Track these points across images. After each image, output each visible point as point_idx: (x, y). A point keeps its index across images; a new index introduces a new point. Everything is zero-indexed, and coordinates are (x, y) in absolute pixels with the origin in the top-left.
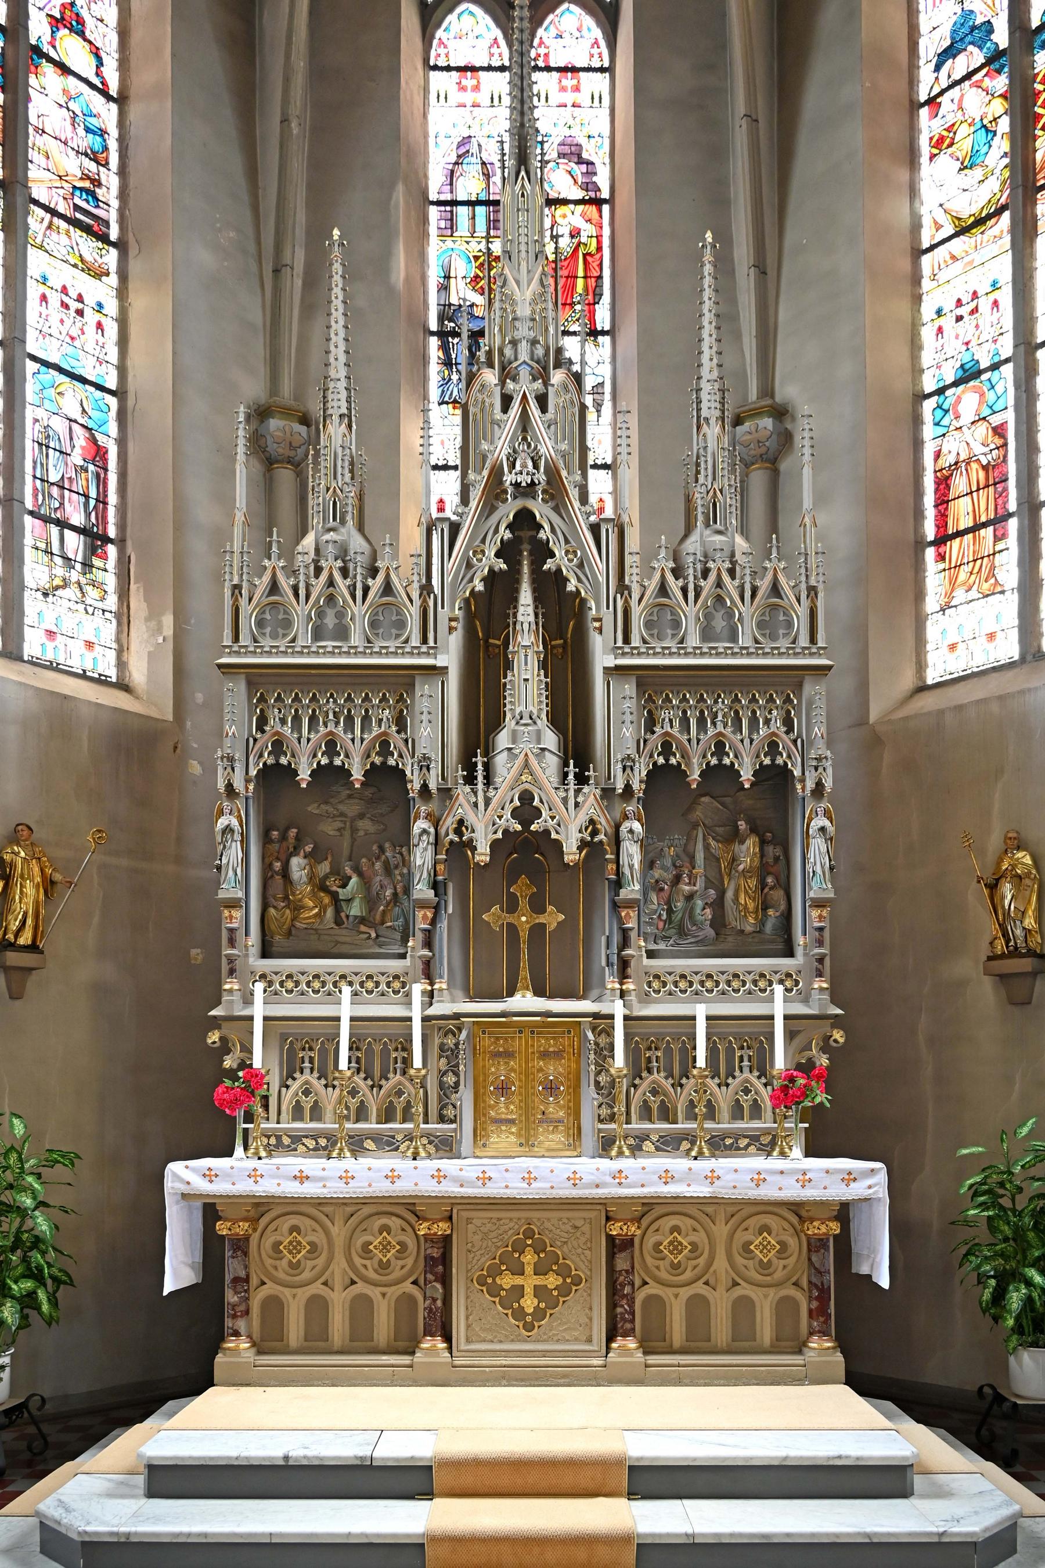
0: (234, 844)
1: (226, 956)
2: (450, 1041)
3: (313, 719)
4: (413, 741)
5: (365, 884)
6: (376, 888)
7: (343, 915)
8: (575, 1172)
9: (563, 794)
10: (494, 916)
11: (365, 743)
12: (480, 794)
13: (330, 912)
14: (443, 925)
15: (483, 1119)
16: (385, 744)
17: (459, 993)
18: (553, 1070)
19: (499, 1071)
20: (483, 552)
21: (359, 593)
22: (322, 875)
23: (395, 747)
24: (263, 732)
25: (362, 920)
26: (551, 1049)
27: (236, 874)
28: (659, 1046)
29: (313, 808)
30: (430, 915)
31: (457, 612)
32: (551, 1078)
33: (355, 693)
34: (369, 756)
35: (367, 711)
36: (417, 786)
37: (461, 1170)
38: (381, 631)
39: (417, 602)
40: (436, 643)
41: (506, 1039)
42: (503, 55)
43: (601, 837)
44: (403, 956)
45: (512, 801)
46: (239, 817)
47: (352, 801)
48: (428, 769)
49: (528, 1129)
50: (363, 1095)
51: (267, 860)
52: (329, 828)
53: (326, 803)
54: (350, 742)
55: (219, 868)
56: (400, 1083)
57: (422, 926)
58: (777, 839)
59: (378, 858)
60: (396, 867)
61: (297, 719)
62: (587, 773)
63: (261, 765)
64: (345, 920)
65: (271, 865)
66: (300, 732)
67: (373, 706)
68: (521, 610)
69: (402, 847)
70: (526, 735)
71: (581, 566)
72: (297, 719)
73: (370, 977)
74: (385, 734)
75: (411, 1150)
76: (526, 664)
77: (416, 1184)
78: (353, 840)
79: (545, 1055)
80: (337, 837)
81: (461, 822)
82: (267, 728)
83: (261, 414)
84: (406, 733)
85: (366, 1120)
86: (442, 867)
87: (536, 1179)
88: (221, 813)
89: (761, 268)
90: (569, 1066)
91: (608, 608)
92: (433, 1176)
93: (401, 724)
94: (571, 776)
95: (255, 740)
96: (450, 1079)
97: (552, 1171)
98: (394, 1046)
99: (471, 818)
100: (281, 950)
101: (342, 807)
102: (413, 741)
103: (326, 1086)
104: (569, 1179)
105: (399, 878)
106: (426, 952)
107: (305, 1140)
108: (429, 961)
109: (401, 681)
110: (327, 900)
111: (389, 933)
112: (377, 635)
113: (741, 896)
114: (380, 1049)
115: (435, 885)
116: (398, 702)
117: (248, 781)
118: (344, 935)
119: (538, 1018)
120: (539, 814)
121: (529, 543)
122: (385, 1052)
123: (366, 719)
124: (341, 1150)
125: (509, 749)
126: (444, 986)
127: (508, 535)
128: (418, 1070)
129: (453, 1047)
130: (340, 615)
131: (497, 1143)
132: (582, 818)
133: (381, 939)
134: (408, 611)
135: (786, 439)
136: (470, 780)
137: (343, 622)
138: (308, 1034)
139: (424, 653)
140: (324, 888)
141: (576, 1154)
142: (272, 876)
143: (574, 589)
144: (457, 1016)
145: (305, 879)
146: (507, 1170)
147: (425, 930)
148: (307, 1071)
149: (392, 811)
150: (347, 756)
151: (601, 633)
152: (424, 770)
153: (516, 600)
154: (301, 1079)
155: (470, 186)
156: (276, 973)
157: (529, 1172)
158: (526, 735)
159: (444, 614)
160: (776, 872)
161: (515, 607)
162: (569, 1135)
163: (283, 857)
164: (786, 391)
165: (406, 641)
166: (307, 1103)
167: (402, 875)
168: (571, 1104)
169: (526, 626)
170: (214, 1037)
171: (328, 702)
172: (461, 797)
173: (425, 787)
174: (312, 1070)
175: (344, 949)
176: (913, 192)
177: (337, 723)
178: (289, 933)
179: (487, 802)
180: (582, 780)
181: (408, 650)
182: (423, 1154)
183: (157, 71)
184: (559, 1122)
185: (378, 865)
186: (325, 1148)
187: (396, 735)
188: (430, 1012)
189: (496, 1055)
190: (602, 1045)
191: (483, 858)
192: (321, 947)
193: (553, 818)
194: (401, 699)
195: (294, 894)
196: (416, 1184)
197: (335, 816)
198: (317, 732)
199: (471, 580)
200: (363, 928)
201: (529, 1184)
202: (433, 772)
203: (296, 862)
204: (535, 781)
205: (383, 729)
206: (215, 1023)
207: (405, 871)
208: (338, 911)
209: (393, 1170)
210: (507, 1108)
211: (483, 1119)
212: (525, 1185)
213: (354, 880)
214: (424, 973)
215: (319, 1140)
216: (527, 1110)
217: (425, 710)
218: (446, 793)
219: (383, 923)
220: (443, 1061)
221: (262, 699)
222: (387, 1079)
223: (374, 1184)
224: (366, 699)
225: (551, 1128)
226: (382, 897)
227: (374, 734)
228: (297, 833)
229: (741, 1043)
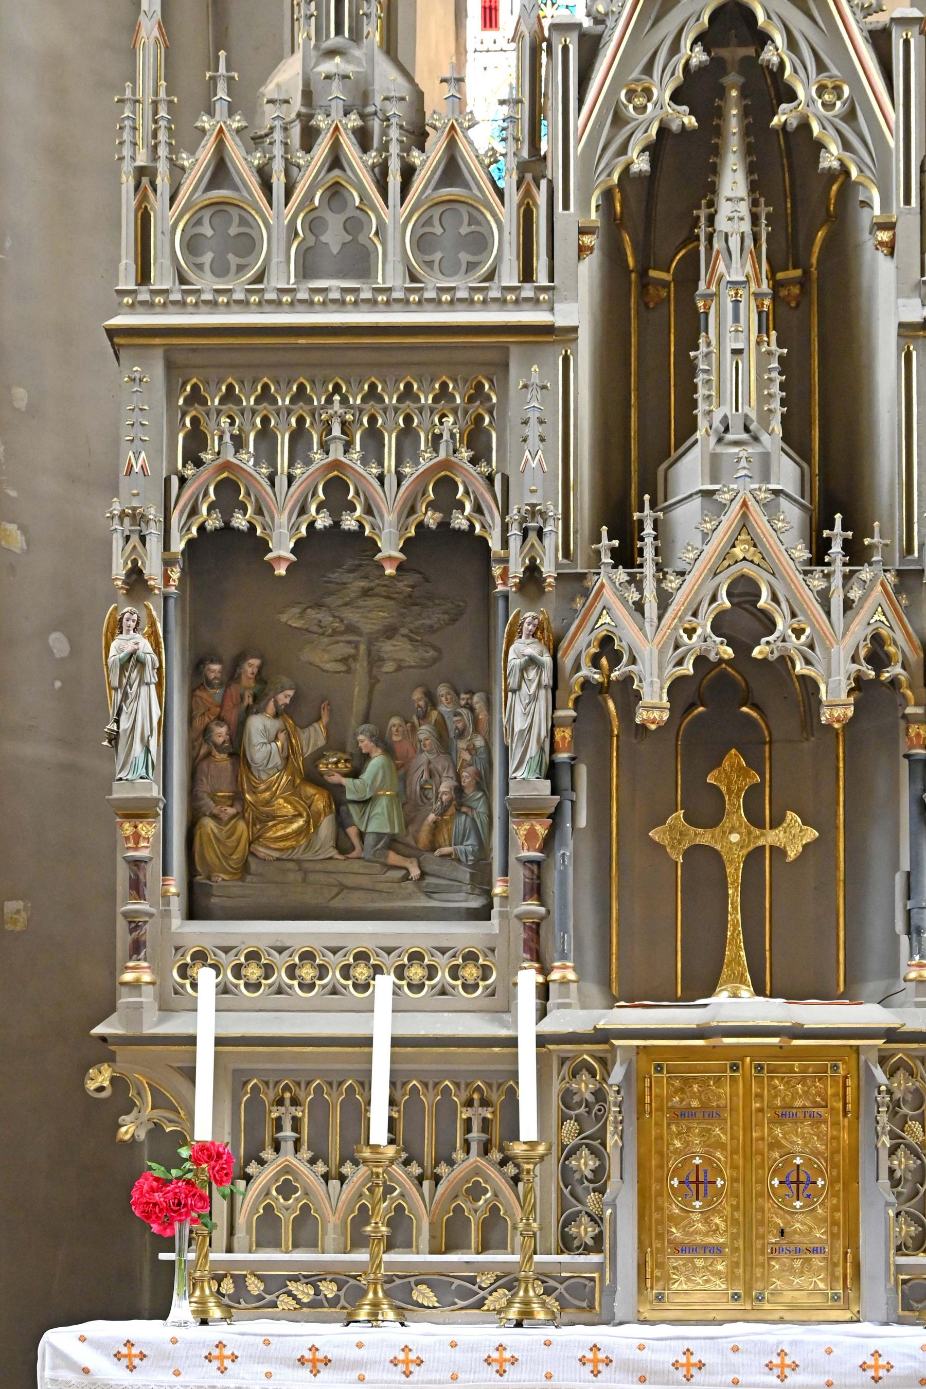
0: (144, 689)
1: (126, 915)
2: (585, 1087)
3: (299, 436)
4: (506, 480)
5: (398, 768)
6: (418, 776)
7: (352, 832)
8: (876, 1354)
9: (818, 583)
10: (674, 834)
11: (405, 484)
12: (650, 586)
13: (327, 826)
14: (566, 851)
15: (657, 1244)
16: (446, 486)
17: (593, 990)
18: (802, 1143)
19: (689, 1145)
20: (648, 92)
21: (394, 180)
22: (308, 751)
23: (467, 492)
24: (199, 463)
25: (392, 842)
26: (798, 1103)
27: (148, 751)
29: (291, 618)
30: (541, 830)
31: (593, 215)
32: (798, 1161)
33: (384, 382)
34: (412, 511)
35: (408, 419)
36: (517, 569)
37: (641, 1348)
38: (437, 256)
39: (513, 197)
40: (551, 280)
41: (704, 1082)
43: (895, 670)
44: (483, 914)
45: (714, 599)
46: (152, 636)
47: (371, 602)
48: (540, 533)
49: (749, 1265)
50: (402, 1195)
51: (199, 723)
52: (324, 657)
53: (319, 606)
54: (376, 483)
55: (114, 738)
56: (477, 1171)
57: (525, 854)
59: (424, 717)
60: (461, 734)
61: (266, 435)
62: (867, 541)
63: (194, 530)
64: (356, 840)
65: (206, 732)
66: (273, 463)
67: (421, 410)
68: (725, 209)
69: (472, 693)
70: (743, 463)
71: (850, 116)
72: (266, 435)
73: (416, 957)
74: (446, 464)
75: (516, 1307)
76: (736, 319)
77: (549, 1377)
78: (373, 680)
79: (784, 1115)
81: (607, 642)
82: (207, 457)
84: (489, 463)
85: (408, 1245)
86: (568, 733)
87: (795, 1367)
88: (117, 627)
90: (835, 1138)
91: (907, 201)
92: (583, 1361)
93: (477, 442)
94: (836, 548)
95: (183, 480)
96: (585, 1163)
97: (829, 1352)
98: (464, 1095)
99: (629, 634)
100: (228, 903)
101: (351, 615)
102: (506, 480)
103: (326, 1177)
104: (864, 1367)
105: (467, 756)
106: (533, 907)
107: (292, 1286)
108: (538, 925)
109: (479, 361)
110: (320, 802)
111: (446, 868)
112: (430, 264)
114: (455, 1099)
115: (551, 772)
116: (471, 399)
117: (168, 563)
118: (353, 869)
119: (775, 1041)
120: (770, 626)
121: (741, 72)
122: (445, 1110)
123: (407, 434)
124: (376, 1305)
125: (707, 494)
126: (571, 976)
127: (699, 57)
128: (532, 1145)
129: (591, 1098)
130: (354, 225)
131: (686, 1292)
132: (858, 633)
133: (430, 880)
134: (494, 215)
136: (626, 557)
137: (361, 239)
138: (287, 1072)
139: (527, 300)
140: (315, 779)
141: (848, 1315)
142: (209, 754)
143: (835, 164)
144: (603, 1036)
145: (277, 760)
146: (735, 1349)
147: (531, 862)
148: (288, 1146)
149: (453, 621)
150: (369, 511)
151: (891, 254)
152: (533, 536)
153: (713, 189)
154: (275, 1163)
156: (226, 950)
157: (782, 1354)
158: (743, 463)
159: (568, 220)
161: (711, 204)
162: (834, 1278)
163: (232, 715)
165: (490, 276)
166: (287, 1211)
167: (471, 750)
168: (839, 1215)
169: (734, 243)
170: (100, 1078)
171: (329, 401)
172: (608, 592)
173: (533, 571)
174: (297, 1144)
175: (357, 901)
177: (348, 447)
178: (245, 869)
179: (664, 600)
180: (856, 553)
181: (494, 294)
182: (541, 1315)
184: (815, 1250)
185: (425, 731)
186: (333, 1302)
187: (469, 467)
188: (550, 1025)
189: (684, 1114)
190: (898, 1095)
191: (656, 714)
192: (310, 897)
193: (798, 632)
194: (477, 395)
195: (254, 791)
196: (549, 1377)
197: (335, 633)
198: (308, 462)
199: (623, 150)
200: (393, 858)
201: (782, 1377)
202: (548, 541)
203: (259, 725)
204: (766, 562)
205: (442, 455)
206: (105, 1049)
207: (479, 742)
208: (341, 823)
209: (500, 1348)
210: (707, 1221)
211: (657, 1244)
212: (773, 1379)
213: (377, 761)
214: (527, 948)
215: (323, 1286)
216: (747, 1227)
217: (533, 416)
218: (575, 583)
219: (433, 847)
220: (570, 1126)
221: (196, 398)
222: (451, 1163)
223: (461, 1376)
224: (408, 394)
225: (797, 1264)
226: (431, 795)
227: (424, 465)
228: (260, 668)
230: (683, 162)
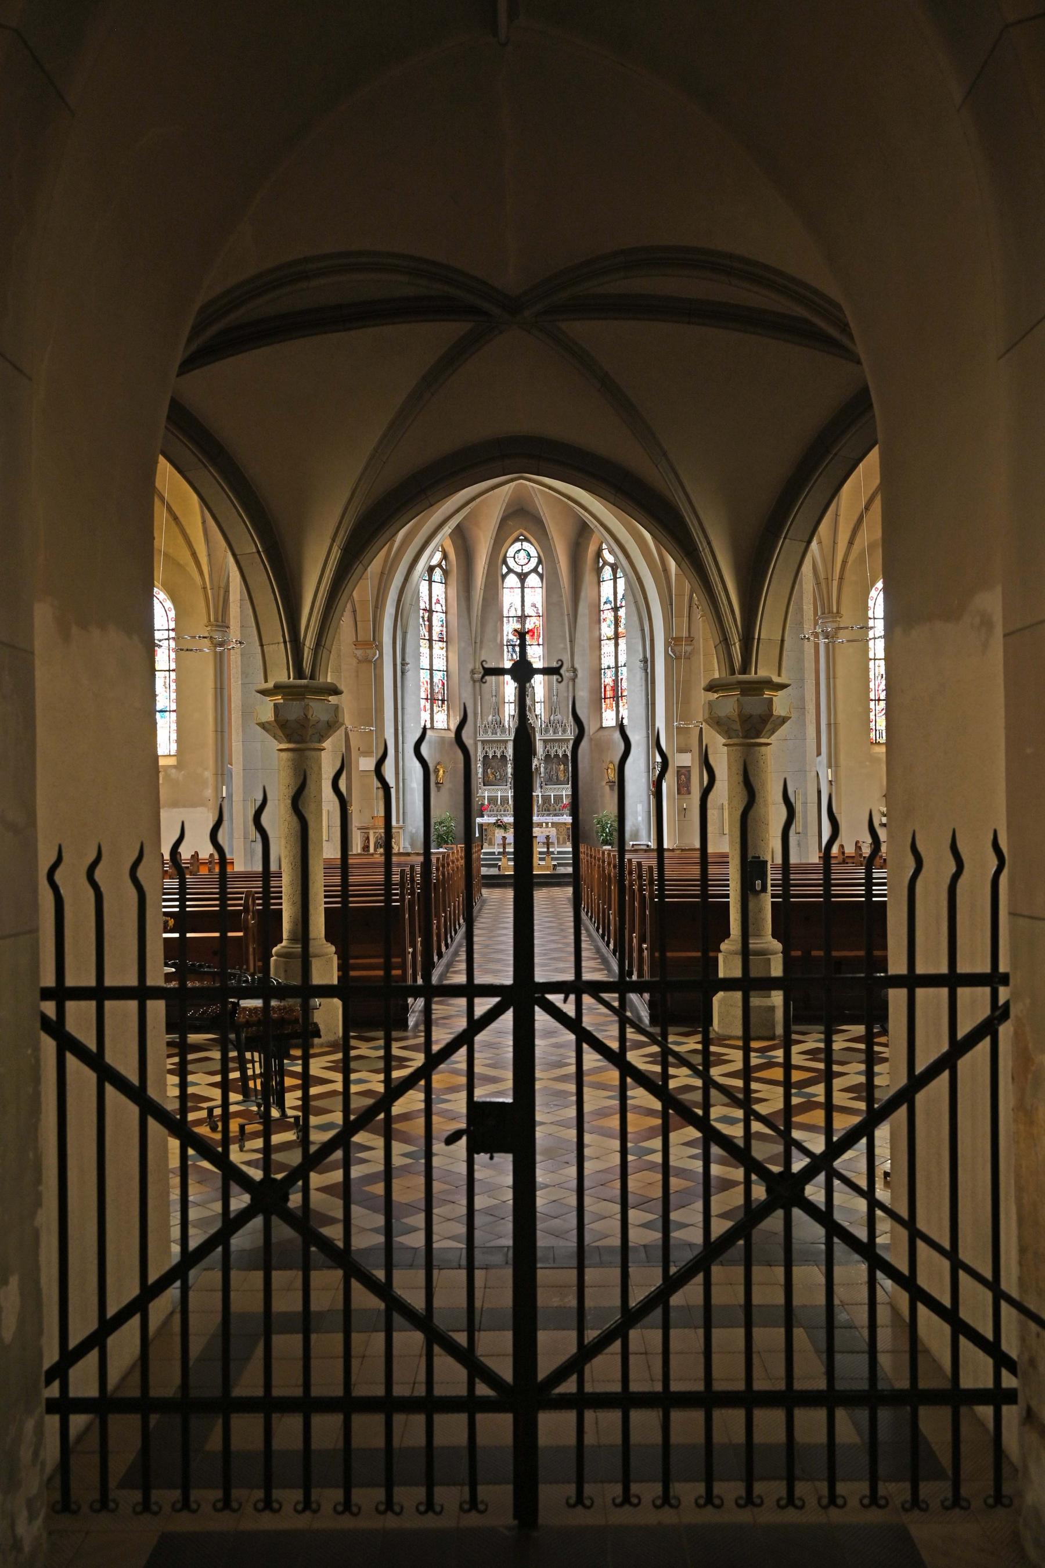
42: (519, 585)
89: (571, 641)
109: (506, 741)
135: (576, 676)
155: (512, 613)
164: (577, 666)
176: (600, 629)
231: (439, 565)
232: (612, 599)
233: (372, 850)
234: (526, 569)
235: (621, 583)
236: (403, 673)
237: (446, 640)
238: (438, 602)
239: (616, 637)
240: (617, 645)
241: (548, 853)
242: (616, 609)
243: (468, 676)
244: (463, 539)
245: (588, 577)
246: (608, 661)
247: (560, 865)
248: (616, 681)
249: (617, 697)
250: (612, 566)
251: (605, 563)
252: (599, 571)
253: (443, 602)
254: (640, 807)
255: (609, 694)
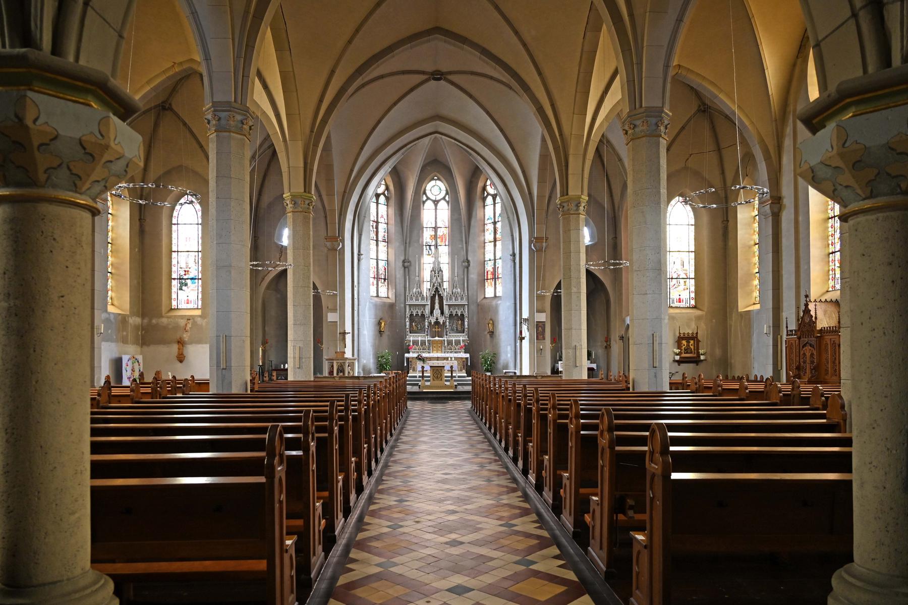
28: (450, 343)
58: (463, 321)
80: (417, 322)
83: (404, 262)
109: (424, 305)
113: (459, 327)
114: (423, 343)
160: (463, 324)
164: (469, 258)
183: (392, 222)
229: (457, 342)
230: (434, 296)
231: (383, 194)
232: (492, 216)
233: (335, 374)
234: (438, 198)
235: (499, 207)
236: (359, 260)
237: (388, 241)
238: (382, 217)
239: (495, 240)
240: (495, 246)
241: (452, 377)
242: (495, 223)
243: (401, 264)
244: (397, 176)
245: (479, 203)
246: (489, 255)
247: (459, 384)
248: (494, 268)
249: (495, 278)
250: (492, 196)
251: (488, 194)
252: (484, 199)
253: (385, 217)
254: (509, 348)
255: (490, 276)
